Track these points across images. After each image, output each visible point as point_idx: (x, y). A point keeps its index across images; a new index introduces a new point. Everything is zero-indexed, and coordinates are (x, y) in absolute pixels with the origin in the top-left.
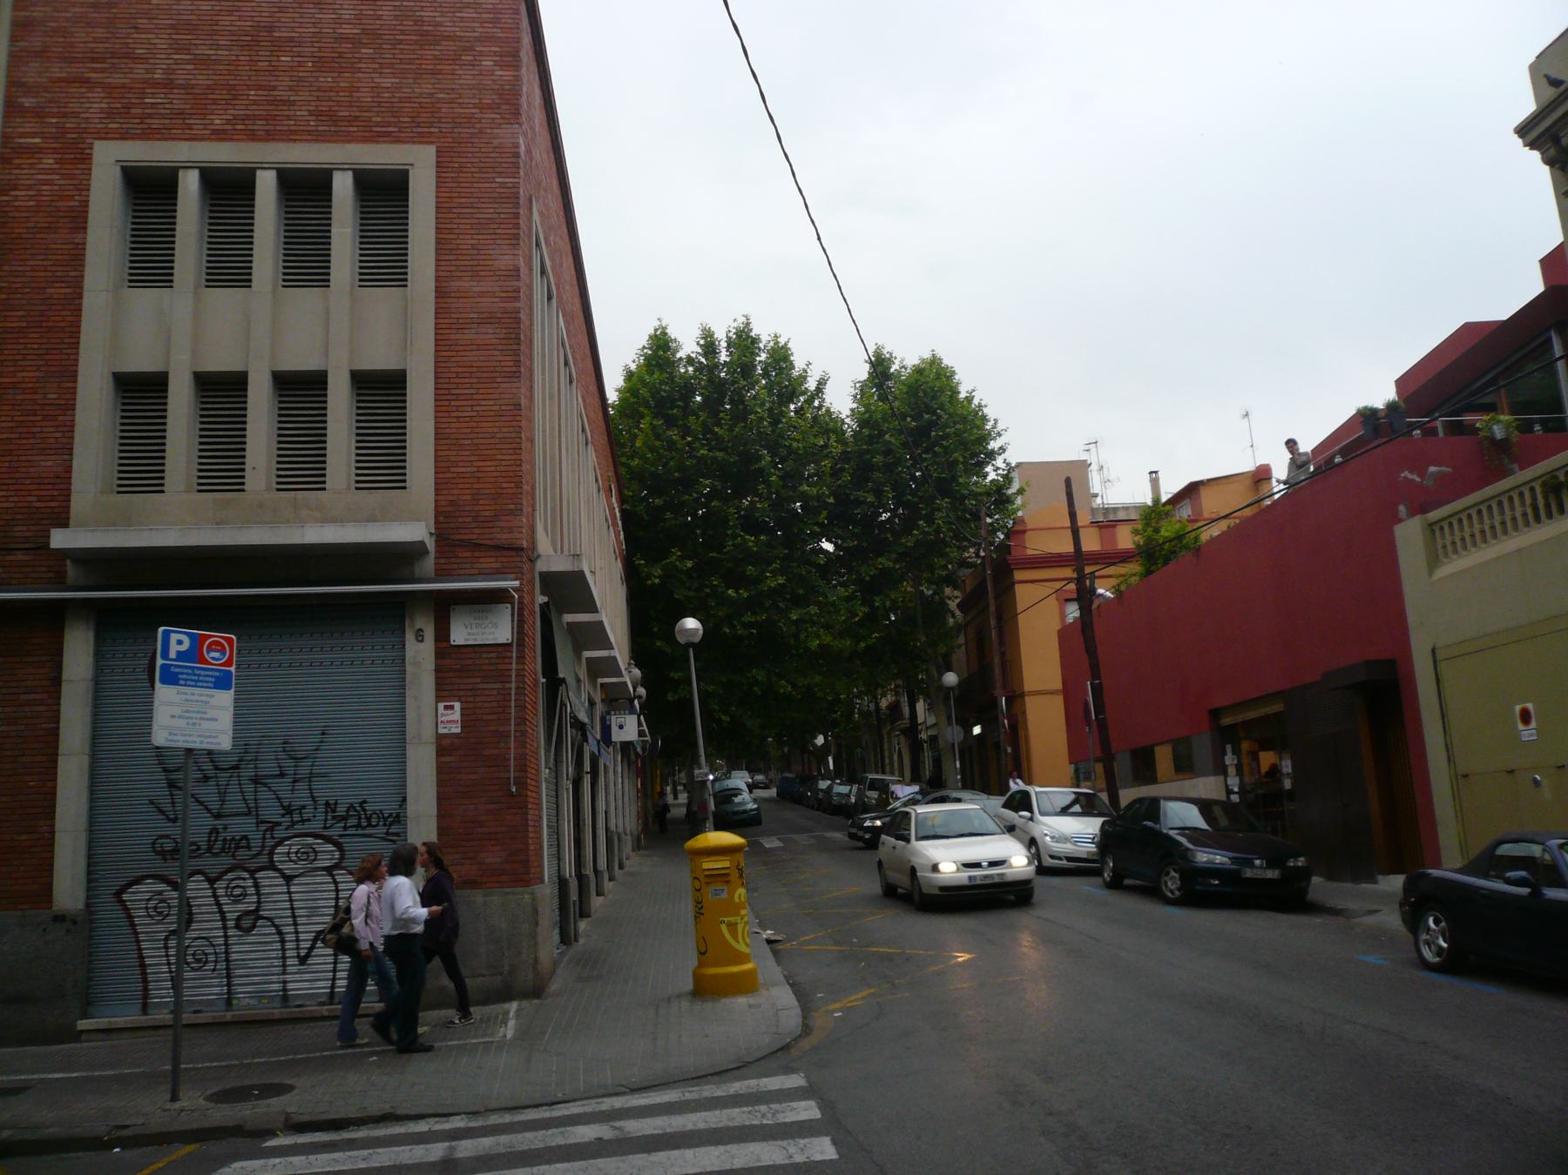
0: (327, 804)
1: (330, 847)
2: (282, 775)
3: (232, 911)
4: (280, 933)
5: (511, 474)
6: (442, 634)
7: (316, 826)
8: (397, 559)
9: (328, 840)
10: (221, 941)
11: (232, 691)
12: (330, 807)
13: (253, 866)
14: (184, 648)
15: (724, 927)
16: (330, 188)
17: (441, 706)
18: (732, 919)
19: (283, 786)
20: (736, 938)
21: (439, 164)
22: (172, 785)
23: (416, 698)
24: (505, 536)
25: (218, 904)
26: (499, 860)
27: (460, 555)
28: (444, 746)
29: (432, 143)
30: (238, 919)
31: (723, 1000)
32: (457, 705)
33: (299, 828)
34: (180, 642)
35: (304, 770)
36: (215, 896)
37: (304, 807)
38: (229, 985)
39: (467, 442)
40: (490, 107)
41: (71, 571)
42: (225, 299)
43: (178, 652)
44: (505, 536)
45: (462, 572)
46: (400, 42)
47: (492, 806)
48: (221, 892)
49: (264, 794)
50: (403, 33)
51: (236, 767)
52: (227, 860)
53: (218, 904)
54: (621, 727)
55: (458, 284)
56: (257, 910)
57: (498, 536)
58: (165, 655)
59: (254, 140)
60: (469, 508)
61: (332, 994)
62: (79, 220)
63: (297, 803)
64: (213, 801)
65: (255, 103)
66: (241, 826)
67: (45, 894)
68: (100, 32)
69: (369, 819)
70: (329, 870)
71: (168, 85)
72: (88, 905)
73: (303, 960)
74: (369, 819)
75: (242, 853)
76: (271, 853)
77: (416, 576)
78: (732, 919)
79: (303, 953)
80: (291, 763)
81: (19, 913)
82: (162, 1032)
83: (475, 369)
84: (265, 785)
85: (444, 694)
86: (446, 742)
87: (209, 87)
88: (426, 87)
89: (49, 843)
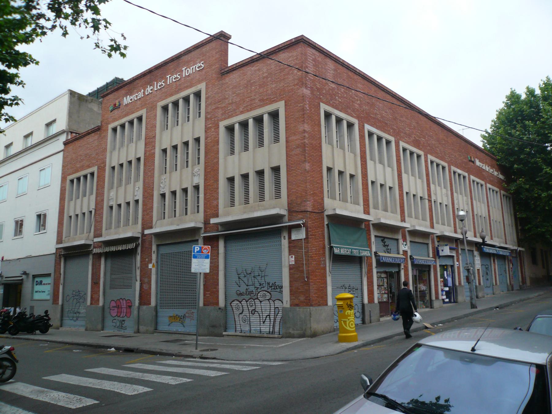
0: (268, 283)
1: (268, 294)
2: (259, 275)
3: (251, 309)
4: (259, 315)
5: (304, 190)
6: (290, 237)
7: (265, 289)
8: (277, 218)
9: (268, 292)
10: (248, 316)
11: (209, 259)
12: (268, 284)
13: (254, 298)
14: (198, 250)
15: (342, 322)
16: (263, 119)
17: (290, 256)
18: (345, 320)
19: (259, 278)
20: (346, 325)
21: (286, 105)
22: (239, 278)
23: (284, 255)
24: (303, 208)
25: (248, 307)
26: (303, 299)
27: (294, 215)
28: (291, 268)
29: (283, 100)
30: (252, 311)
31: (340, 343)
32: (294, 256)
33: (263, 289)
34: (197, 249)
35: (263, 275)
36: (247, 305)
37: (263, 284)
38: (250, 327)
39: (294, 183)
40: (297, 84)
41: (220, 228)
42: (244, 154)
43: (197, 251)
44: (303, 208)
45: (293, 219)
46: (276, 73)
47: (301, 284)
48: (248, 304)
49: (256, 280)
50: (277, 71)
51: (250, 274)
52: (249, 297)
53: (248, 307)
54: (442, 251)
55: (290, 138)
56: (255, 309)
57: (302, 208)
58: (194, 252)
59: (248, 112)
60: (295, 201)
61: (270, 331)
62: (217, 142)
63: (262, 283)
64: (246, 281)
65: (248, 102)
66: (252, 288)
67: (217, 303)
68: (220, 95)
69: (276, 287)
70: (268, 300)
71: (232, 103)
72: (226, 306)
73: (264, 322)
74: (276, 287)
75: (252, 295)
76: (257, 295)
77: (284, 222)
78: (345, 320)
79: (264, 320)
80: (260, 272)
81: (213, 307)
82: (237, 337)
83: (295, 162)
84: (240, 279)
85: (291, 253)
86: (291, 266)
87: (239, 101)
88: (282, 84)
89: (218, 291)
